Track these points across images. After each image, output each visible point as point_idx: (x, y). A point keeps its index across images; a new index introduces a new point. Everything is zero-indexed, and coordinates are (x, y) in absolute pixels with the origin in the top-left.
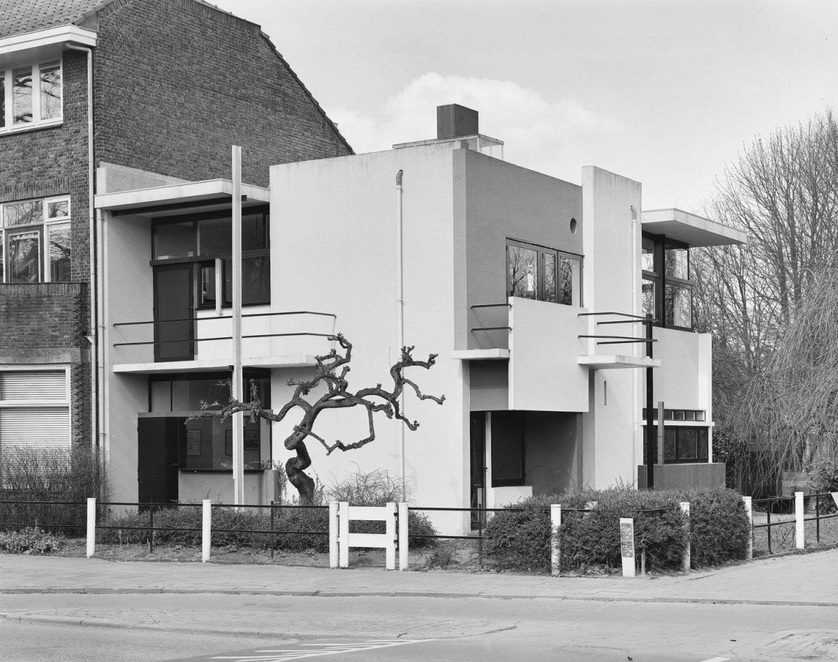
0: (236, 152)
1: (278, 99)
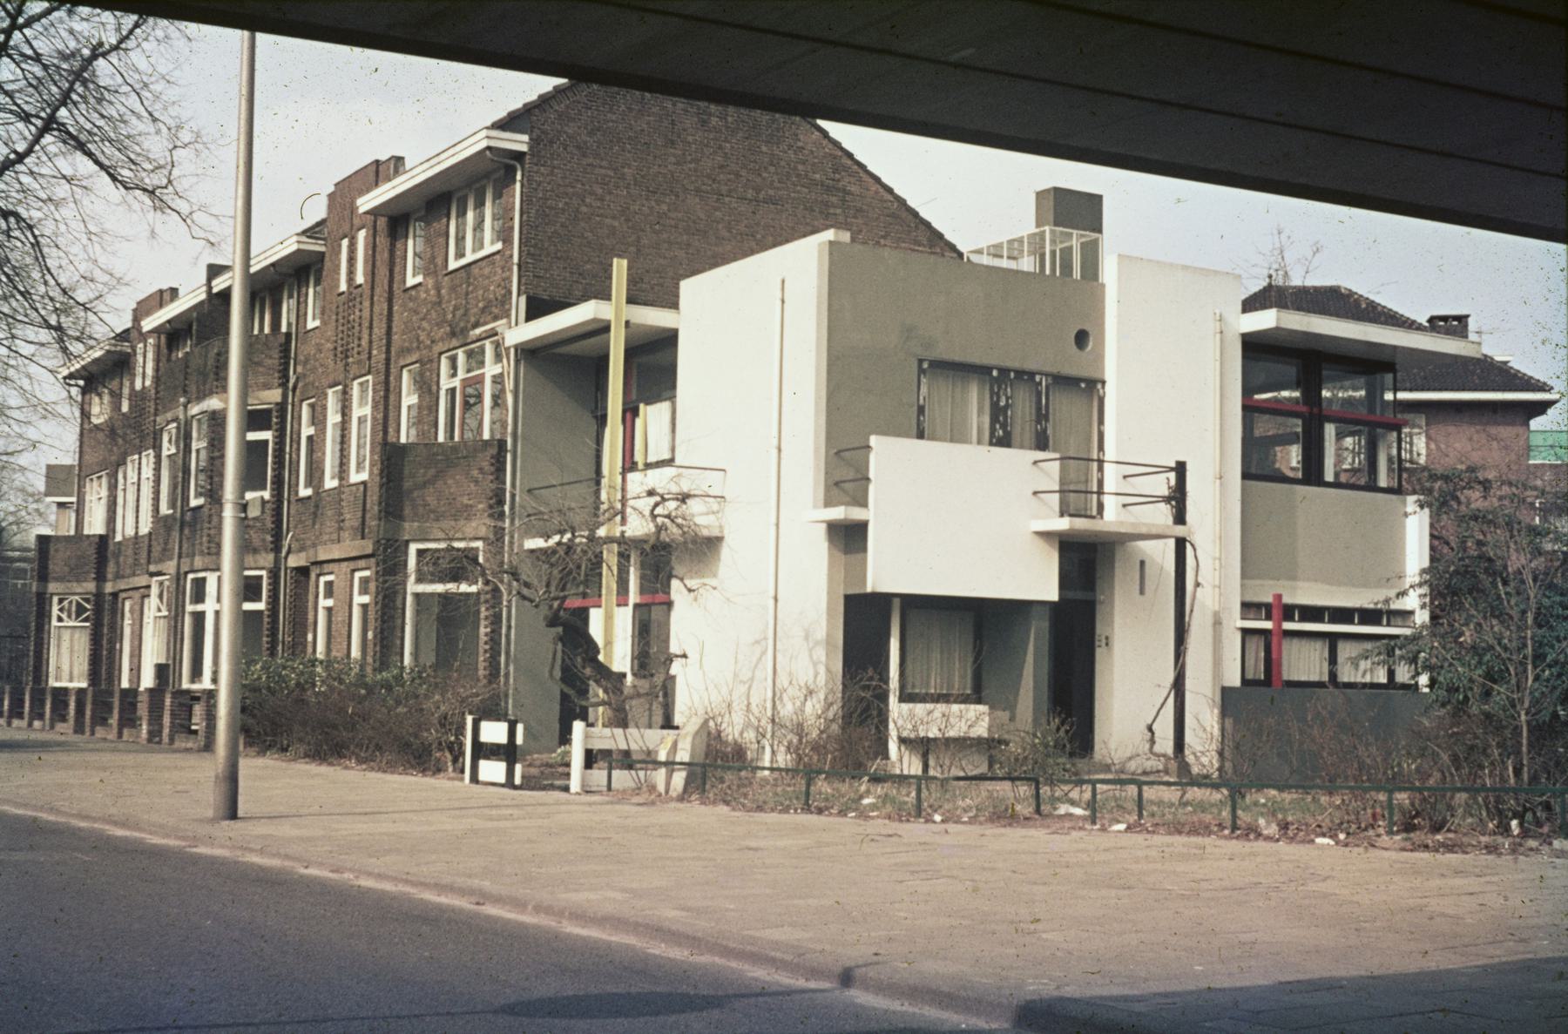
0: (620, 268)
1: (834, 199)
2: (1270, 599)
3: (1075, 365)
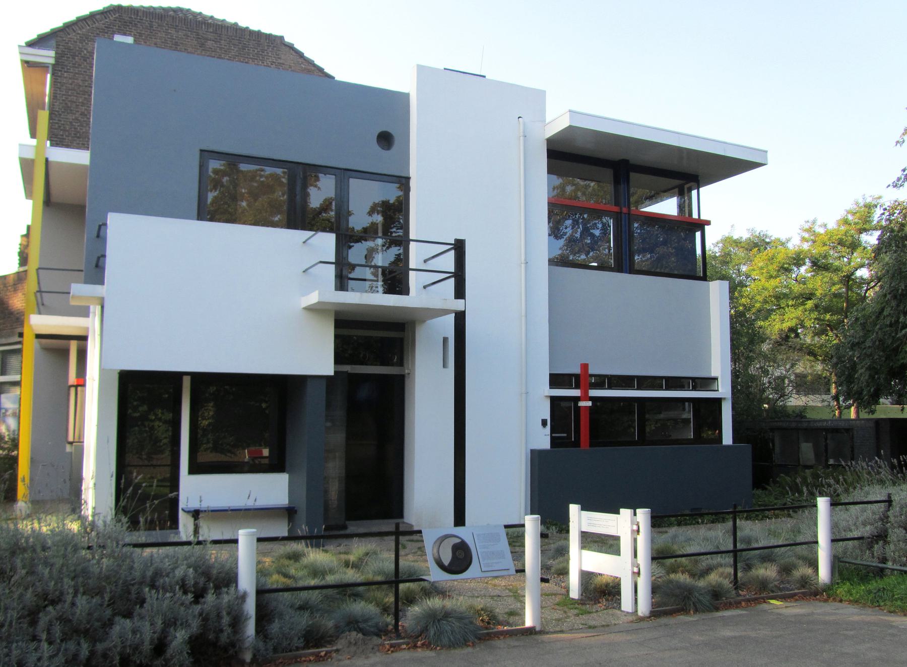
2: (577, 370)
3: (383, 161)
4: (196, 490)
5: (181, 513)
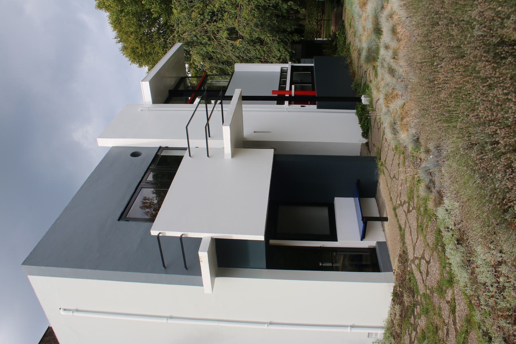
4: (348, 234)
5: (366, 244)
